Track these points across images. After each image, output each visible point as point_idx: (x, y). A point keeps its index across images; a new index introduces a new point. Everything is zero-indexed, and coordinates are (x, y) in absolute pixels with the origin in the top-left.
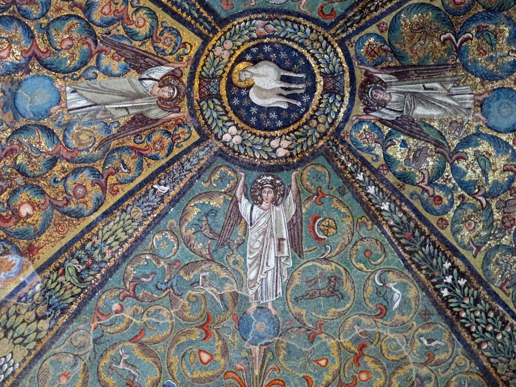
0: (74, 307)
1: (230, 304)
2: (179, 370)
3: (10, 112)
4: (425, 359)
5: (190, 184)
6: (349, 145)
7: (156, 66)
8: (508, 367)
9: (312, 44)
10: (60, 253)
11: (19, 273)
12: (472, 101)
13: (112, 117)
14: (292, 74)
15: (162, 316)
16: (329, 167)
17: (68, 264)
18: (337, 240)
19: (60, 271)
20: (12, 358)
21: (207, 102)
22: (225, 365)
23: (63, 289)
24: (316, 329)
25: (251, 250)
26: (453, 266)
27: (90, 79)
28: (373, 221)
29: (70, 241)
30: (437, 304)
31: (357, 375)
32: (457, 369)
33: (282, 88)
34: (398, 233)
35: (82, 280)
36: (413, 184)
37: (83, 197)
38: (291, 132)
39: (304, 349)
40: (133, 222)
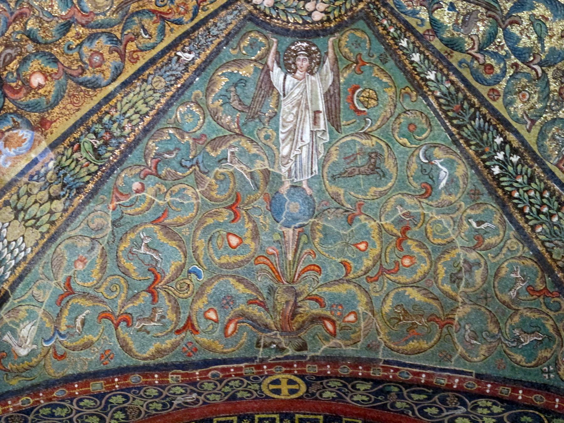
0: (91, 186)
1: (261, 183)
2: (206, 254)
4: (473, 242)
5: (217, 51)
6: (392, 8)
10: (75, 127)
11: (30, 149)
15: (187, 195)
17: (84, 139)
18: (379, 112)
19: (76, 147)
20: (23, 241)
22: (256, 249)
23: (79, 166)
25: (285, 124)
28: (418, 92)
29: (86, 114)
30: (487, 183)
31: (399, 260)
32: (509, 253)
34: (445, 105)
35: (99, 157)
36: (461, 51)
37: (100, 66)
39: (342, 232)
40: (154, 93)
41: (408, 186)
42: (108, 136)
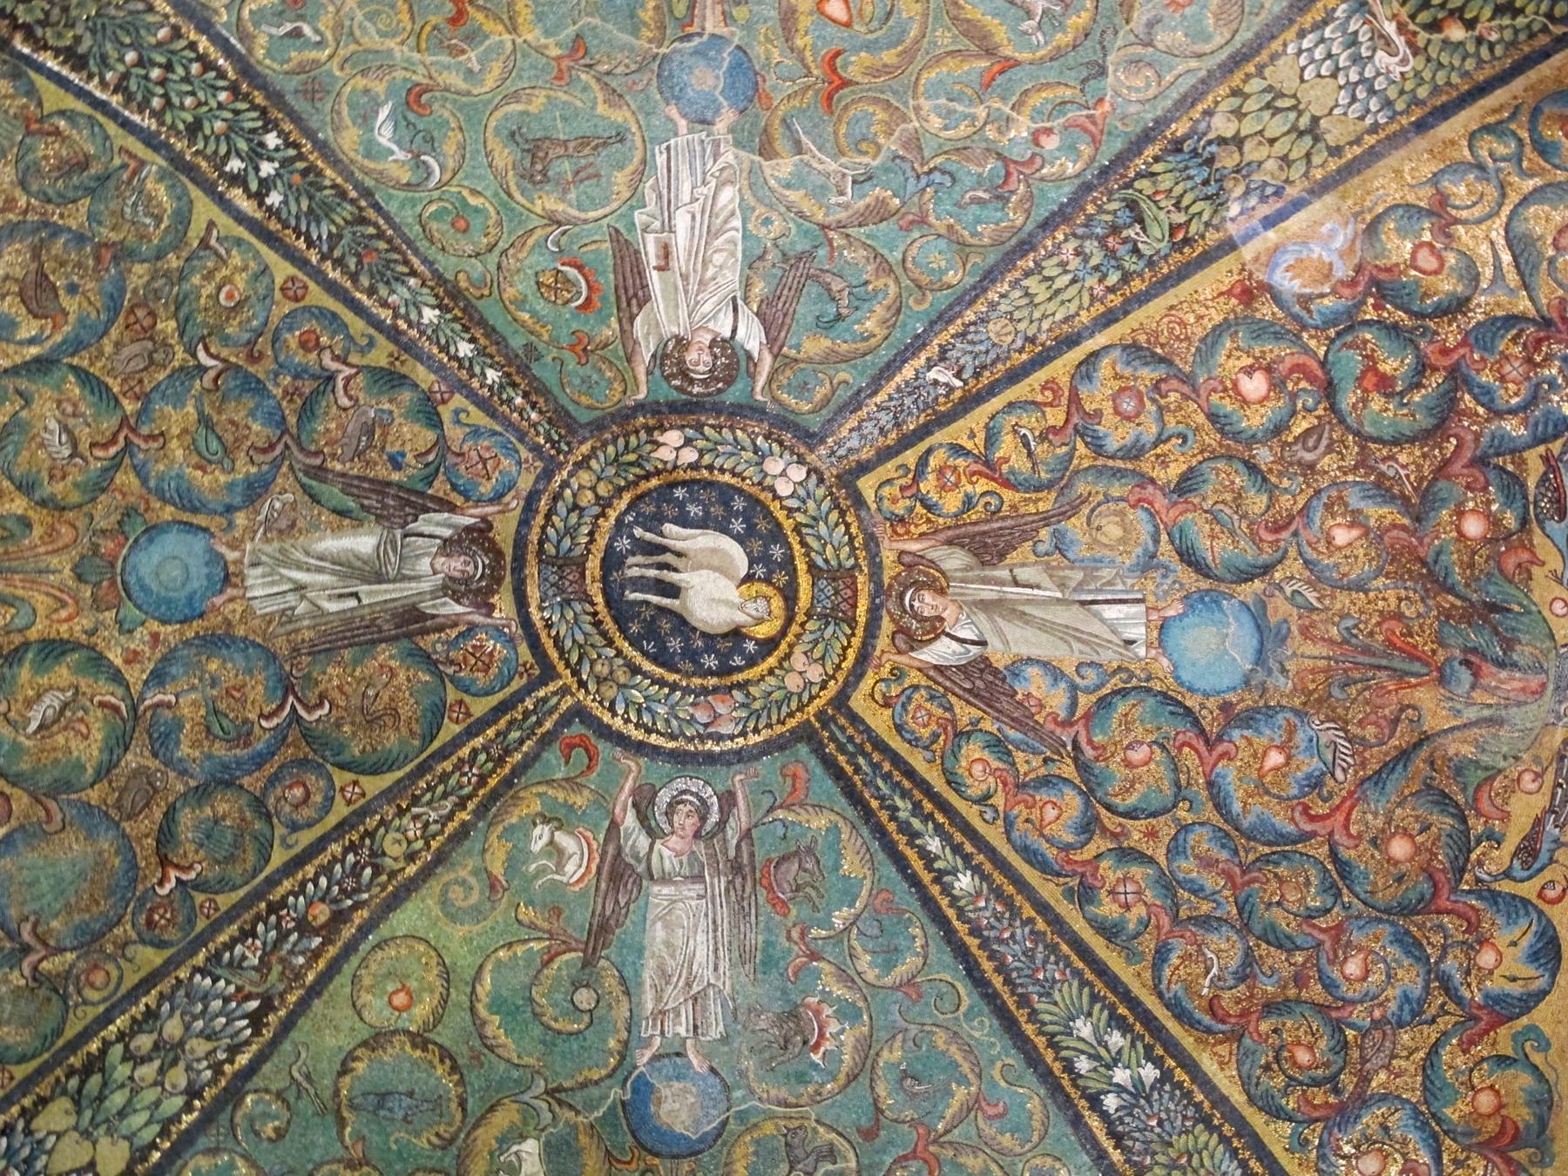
0: (1151, 151)
1: (778, 131)
3: (1273, 620)
6: (521, 440)
7: (948, 668)
11: (1276, 249)
12: (249, 582)
13: (1048, 568)
14: (655, 599)
16: (564, 401)
19: (1180, 236)
20: (1303, 69)
24: (570, 69)
25: (730, 247)
26: (259, 197)
27: (1091, 664)
33: (676, 570)
35: (1132, 205)
37: (1122, 390)
39: (596, 21)
41: (460, 109)
42: (1111, 242)
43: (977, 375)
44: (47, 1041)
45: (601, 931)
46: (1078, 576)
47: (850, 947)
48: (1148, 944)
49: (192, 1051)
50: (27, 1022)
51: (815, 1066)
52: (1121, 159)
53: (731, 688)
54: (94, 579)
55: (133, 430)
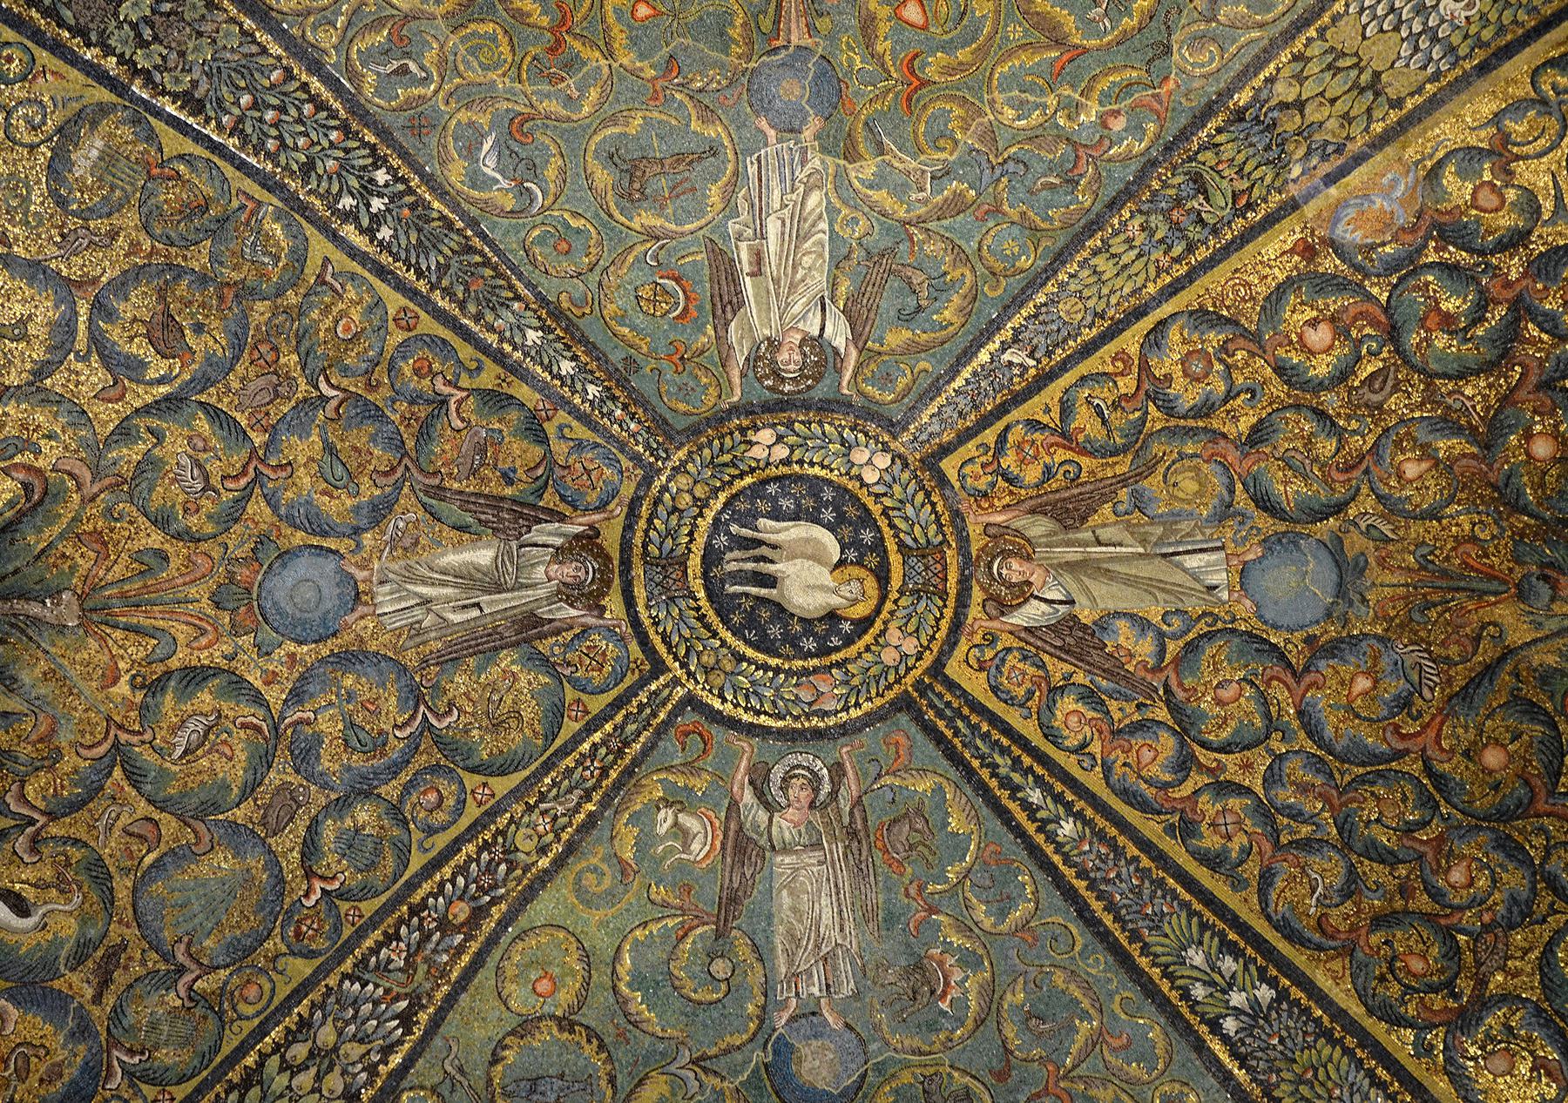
0: (1211, 125)
1: (860, 133)
3: (1350, 554)
6: (622, 451)
8: (214, 41)
9: (718, 662)
11: (1341, 204)
12: (379, 599)
13: (1129, 526)
14: (754, 590)
20: (1364, 27)
21: (928, 541)
29: (1220, 262)
33: (772, 562)
37: (1189, 353)
38: (747, 473)
43: (1049, 354)
44: (205, 1058)
45: (731, 901)
46: (1159, 530)
47: (965, 898)
48: (1252, 869)
49: (347, 1055)
50: (186, 1042)
51: (944, 1013)
52: (1184, 135)
53: (832, 666)
54: (231, 606)
55: (262, 461)
